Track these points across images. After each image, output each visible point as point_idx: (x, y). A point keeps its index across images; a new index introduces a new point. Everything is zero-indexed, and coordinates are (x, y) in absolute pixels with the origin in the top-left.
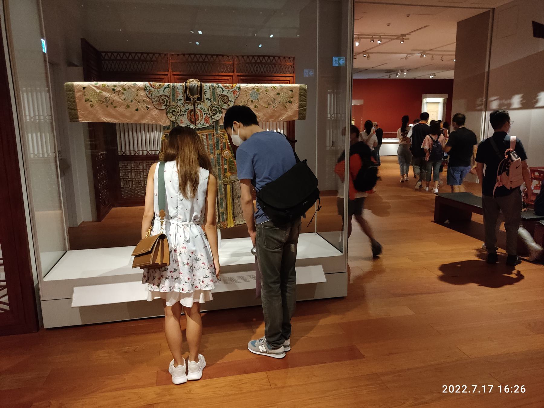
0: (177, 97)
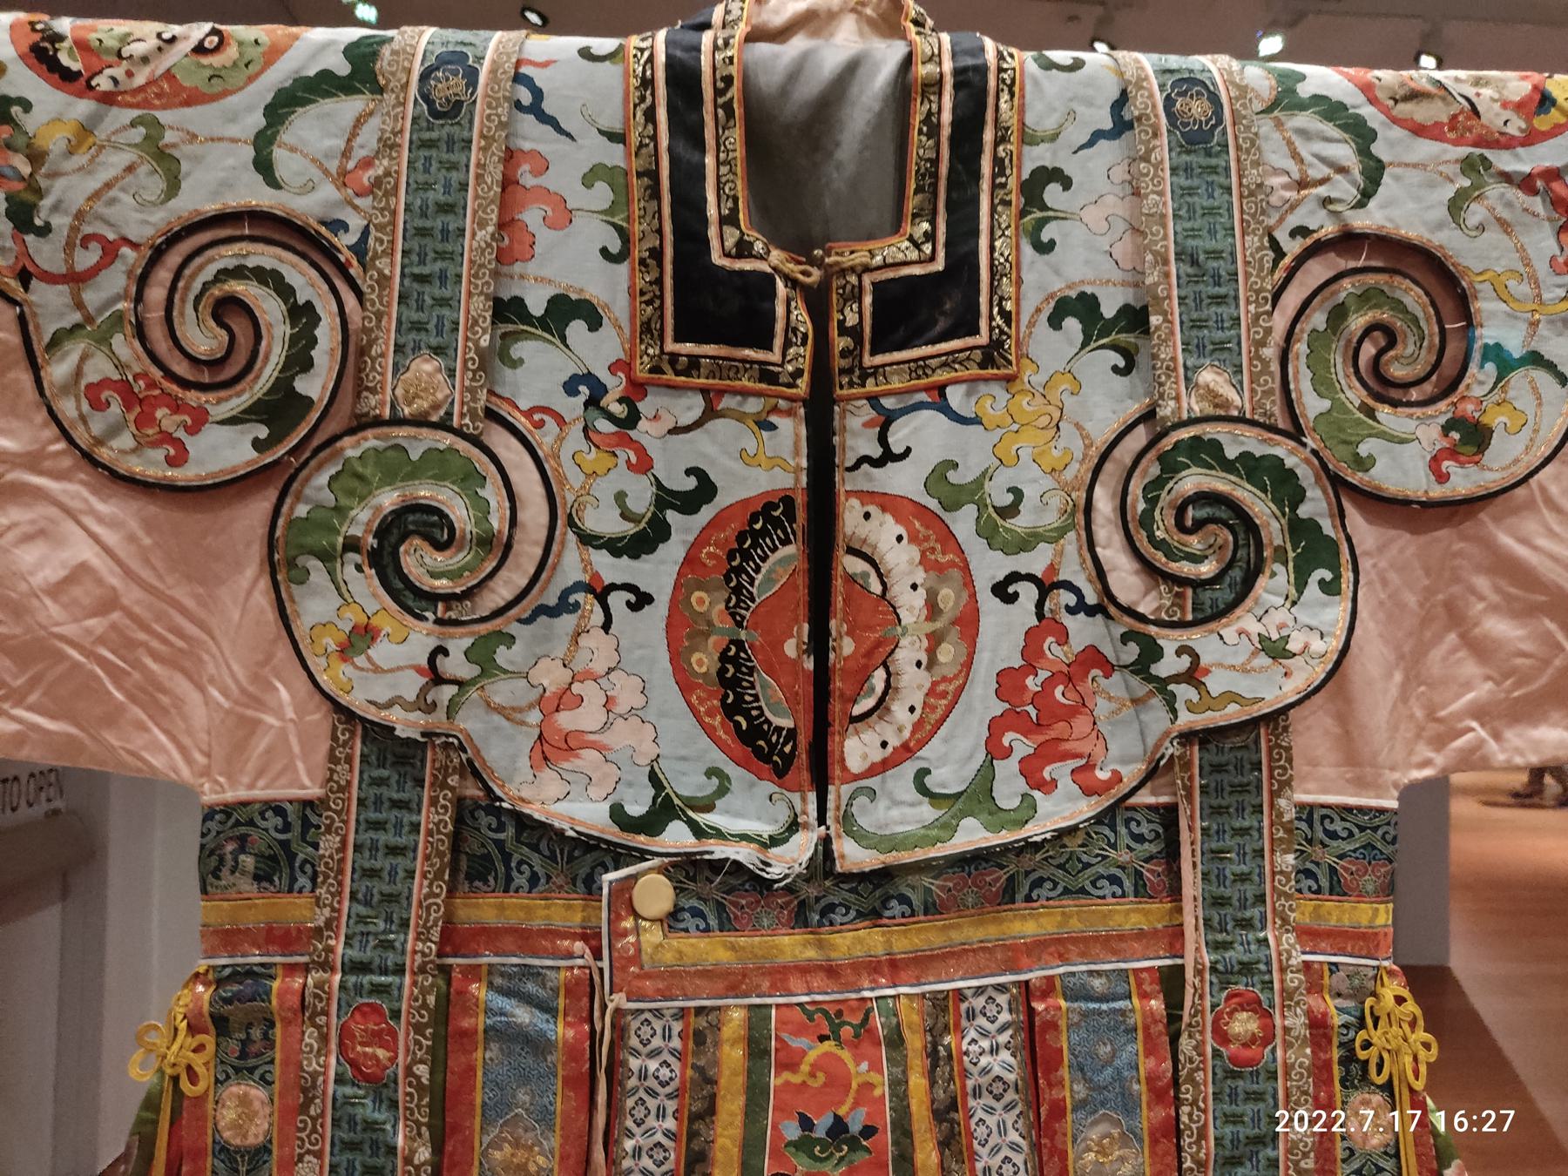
0: (503, 257)
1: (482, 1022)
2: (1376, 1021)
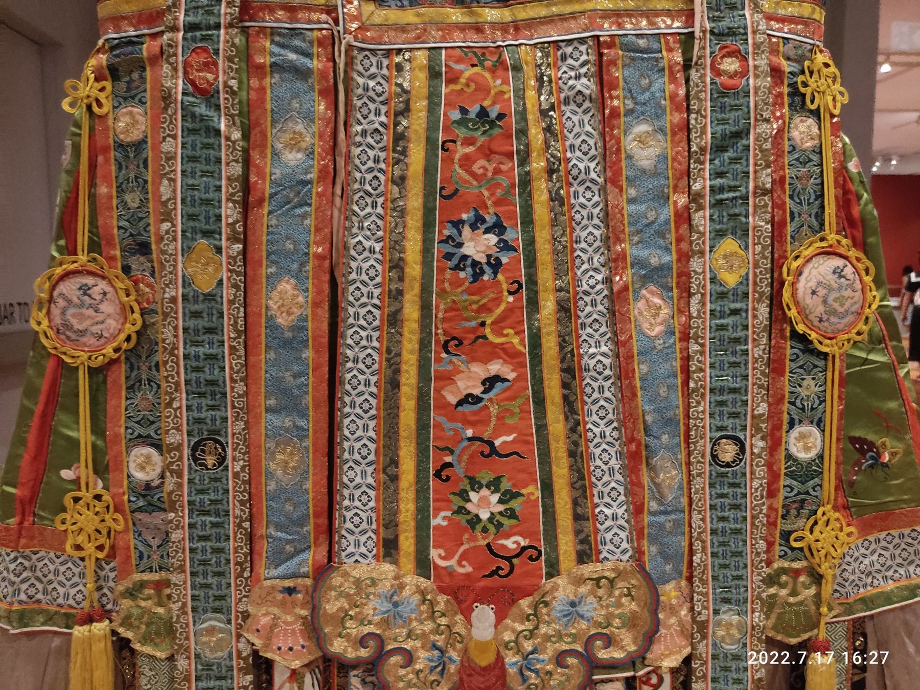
1: (268, 60)
2: (811, 73)
